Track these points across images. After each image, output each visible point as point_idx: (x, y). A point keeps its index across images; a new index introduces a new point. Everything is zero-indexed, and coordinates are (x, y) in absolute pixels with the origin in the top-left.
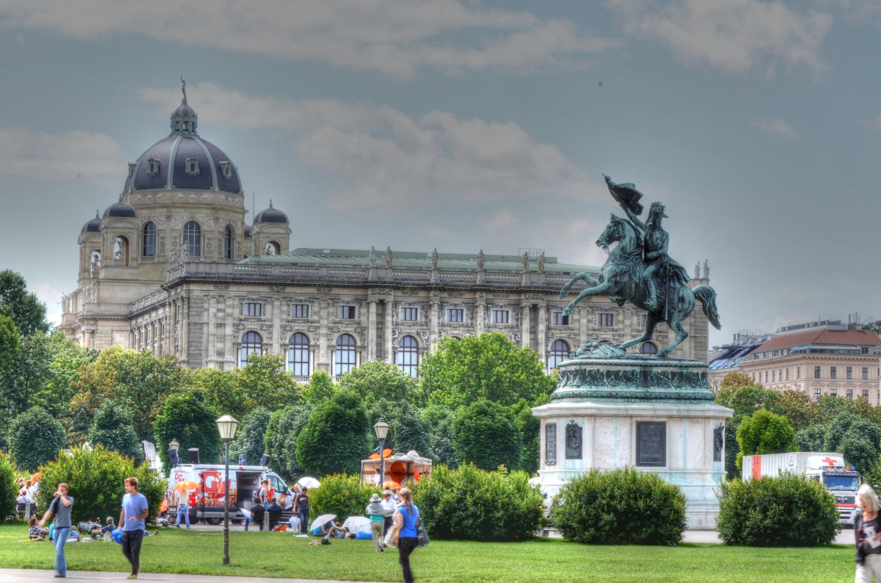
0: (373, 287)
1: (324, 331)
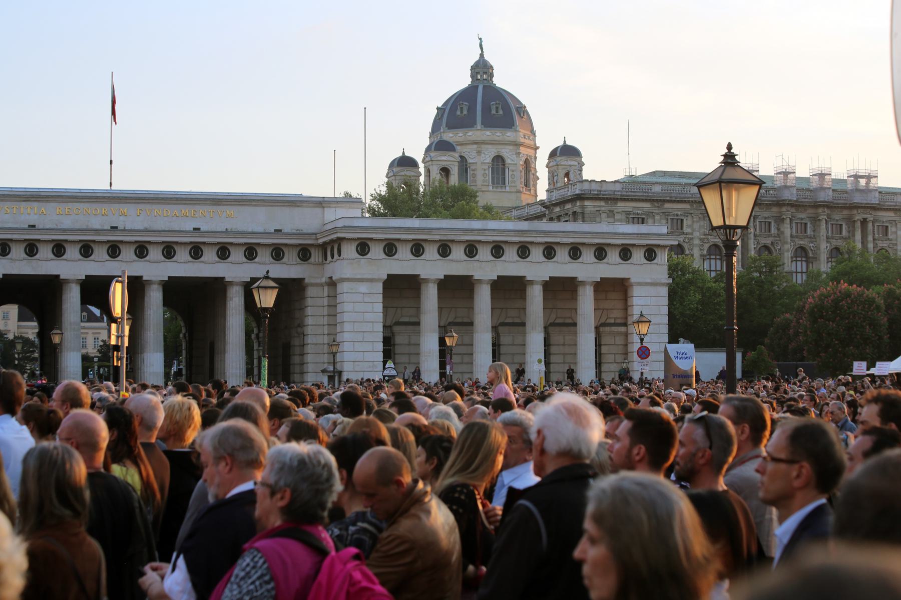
1: (696, 242)
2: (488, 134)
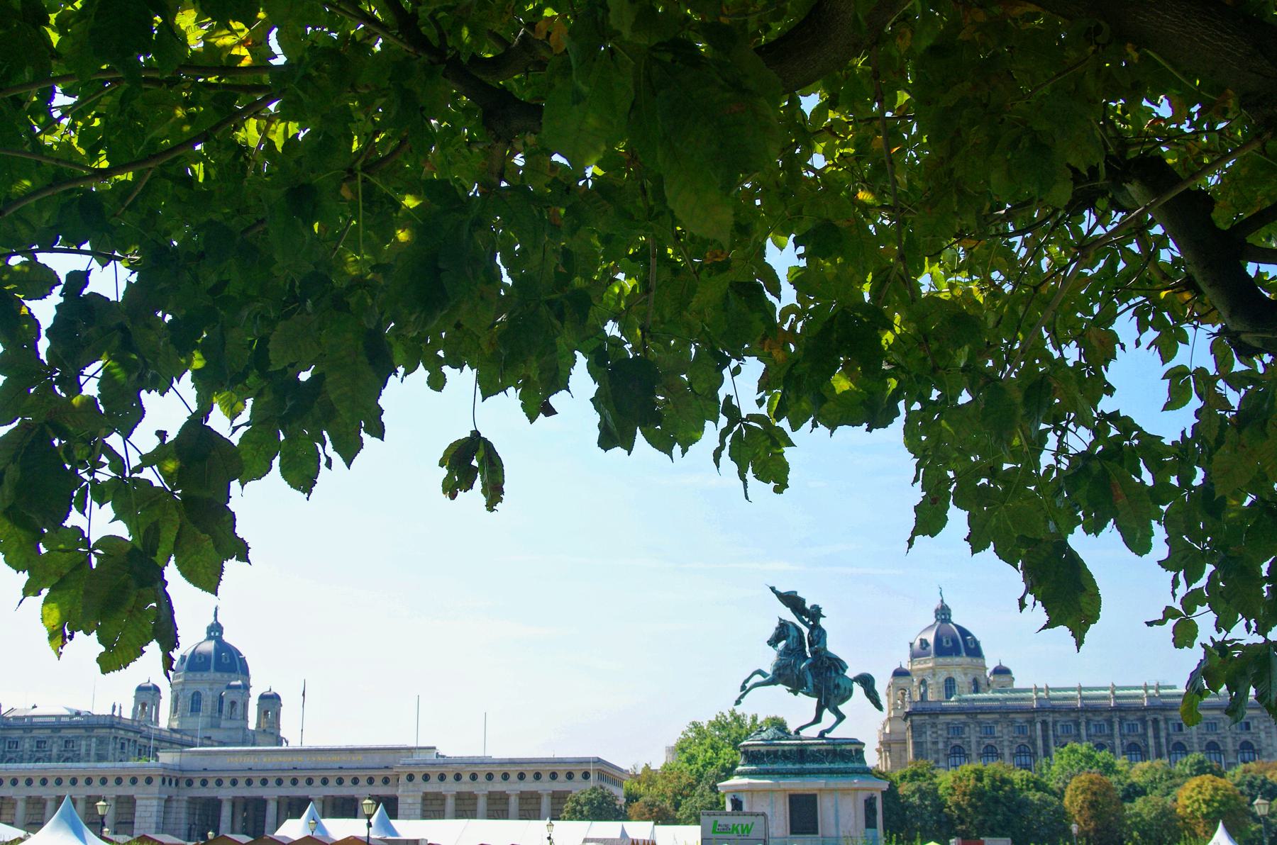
1: (1006, 743)
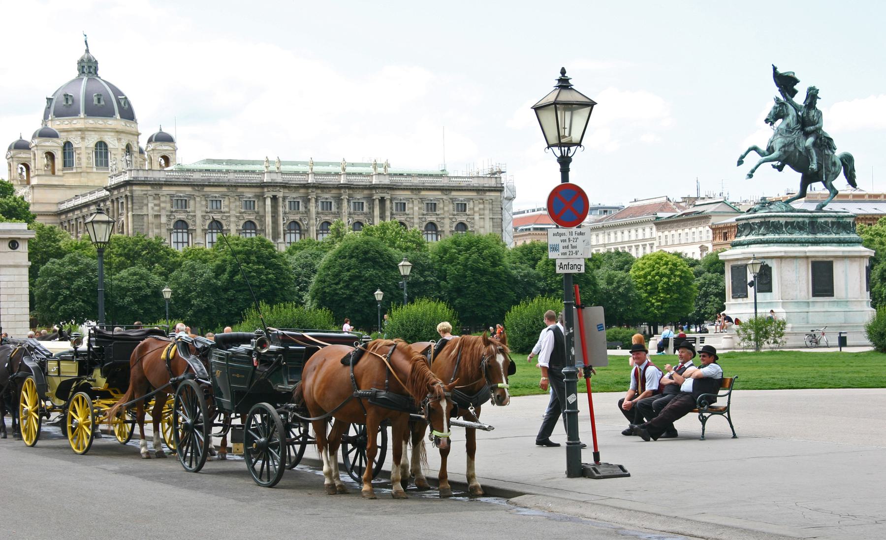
0: (268, 186)
1: (233, 219)
2: (92, 122)
